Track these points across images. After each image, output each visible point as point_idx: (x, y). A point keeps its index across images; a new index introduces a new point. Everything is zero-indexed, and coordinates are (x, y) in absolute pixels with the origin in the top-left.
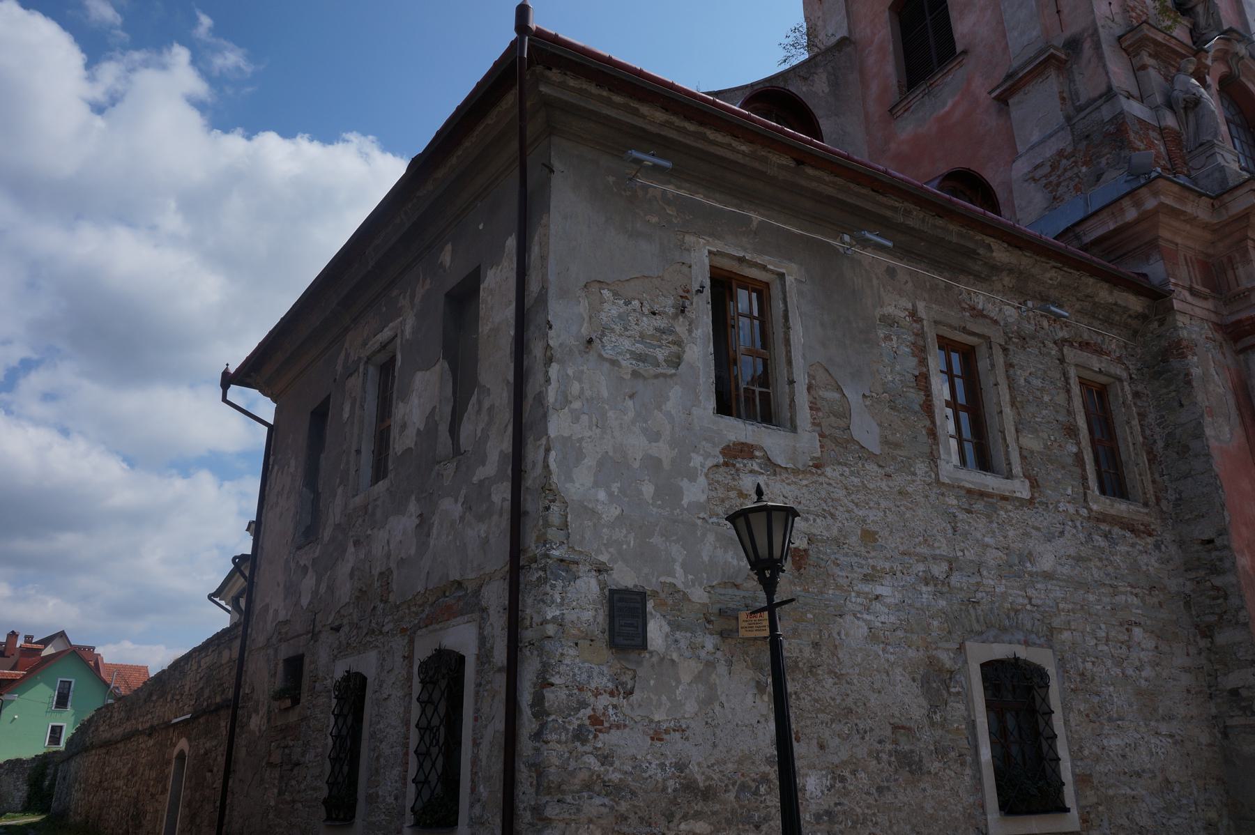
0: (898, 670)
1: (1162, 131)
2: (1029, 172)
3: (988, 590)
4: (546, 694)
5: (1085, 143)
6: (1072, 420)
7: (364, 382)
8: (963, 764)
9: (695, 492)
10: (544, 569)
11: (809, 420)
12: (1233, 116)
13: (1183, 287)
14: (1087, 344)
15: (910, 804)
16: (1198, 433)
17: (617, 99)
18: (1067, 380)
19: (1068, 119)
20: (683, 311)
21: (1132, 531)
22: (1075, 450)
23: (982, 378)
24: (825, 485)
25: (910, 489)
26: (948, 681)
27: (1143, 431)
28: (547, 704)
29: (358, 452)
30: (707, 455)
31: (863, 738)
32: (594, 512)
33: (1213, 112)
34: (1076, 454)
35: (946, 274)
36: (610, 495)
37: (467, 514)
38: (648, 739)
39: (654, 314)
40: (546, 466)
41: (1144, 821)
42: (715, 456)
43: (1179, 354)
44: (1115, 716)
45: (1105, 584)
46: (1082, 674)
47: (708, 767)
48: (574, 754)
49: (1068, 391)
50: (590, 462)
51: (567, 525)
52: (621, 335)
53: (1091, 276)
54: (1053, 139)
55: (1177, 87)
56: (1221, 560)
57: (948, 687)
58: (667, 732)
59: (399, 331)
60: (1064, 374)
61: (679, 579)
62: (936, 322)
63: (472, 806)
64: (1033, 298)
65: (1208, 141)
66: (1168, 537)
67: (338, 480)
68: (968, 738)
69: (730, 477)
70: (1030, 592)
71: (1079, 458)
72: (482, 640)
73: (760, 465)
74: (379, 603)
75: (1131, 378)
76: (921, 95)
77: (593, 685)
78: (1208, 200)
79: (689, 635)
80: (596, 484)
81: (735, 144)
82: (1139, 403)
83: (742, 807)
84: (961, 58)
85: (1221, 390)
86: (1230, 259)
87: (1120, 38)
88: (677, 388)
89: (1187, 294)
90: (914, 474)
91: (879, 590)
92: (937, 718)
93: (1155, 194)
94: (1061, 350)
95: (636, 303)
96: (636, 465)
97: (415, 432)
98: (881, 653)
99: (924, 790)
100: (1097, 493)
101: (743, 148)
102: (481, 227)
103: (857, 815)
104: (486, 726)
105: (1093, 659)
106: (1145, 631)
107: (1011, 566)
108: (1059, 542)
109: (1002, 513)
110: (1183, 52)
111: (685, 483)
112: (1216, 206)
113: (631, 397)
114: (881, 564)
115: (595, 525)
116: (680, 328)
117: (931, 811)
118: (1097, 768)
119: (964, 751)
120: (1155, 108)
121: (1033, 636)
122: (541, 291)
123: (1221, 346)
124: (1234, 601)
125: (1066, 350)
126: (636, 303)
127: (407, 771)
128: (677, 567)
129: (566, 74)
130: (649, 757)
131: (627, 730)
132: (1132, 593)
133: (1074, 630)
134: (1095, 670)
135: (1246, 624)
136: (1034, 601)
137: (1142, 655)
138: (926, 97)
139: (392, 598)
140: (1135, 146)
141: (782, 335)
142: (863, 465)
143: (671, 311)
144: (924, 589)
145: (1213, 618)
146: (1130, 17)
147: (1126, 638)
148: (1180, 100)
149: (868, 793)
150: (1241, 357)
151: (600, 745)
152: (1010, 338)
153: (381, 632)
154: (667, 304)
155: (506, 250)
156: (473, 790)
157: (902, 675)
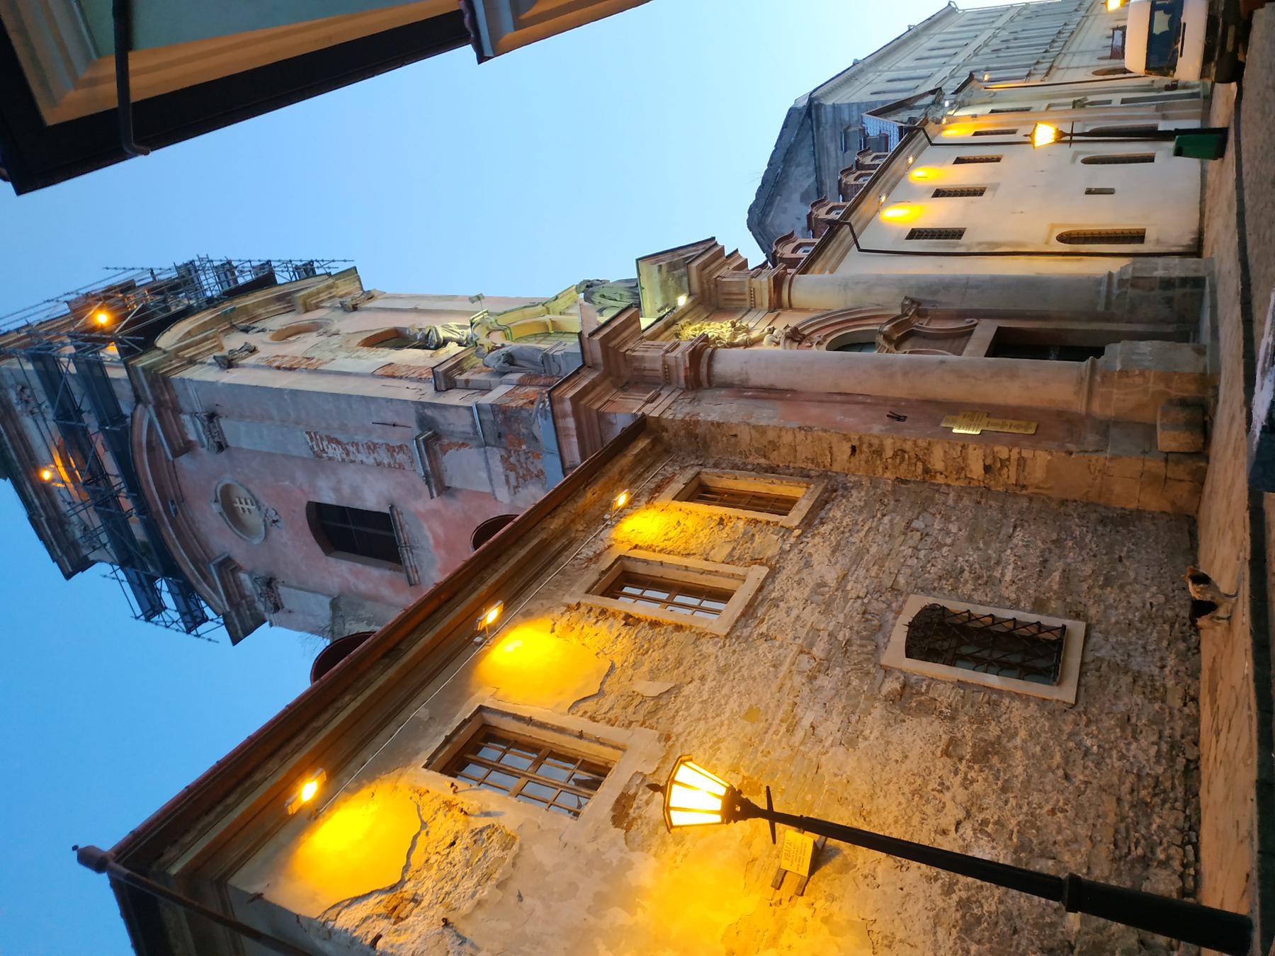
1: (521, 384)
5: (503, 440)
11: (622, 730)
13: (643, 406)
15: (1027, 765)
16: (762, 431)
21: (827, 502)
24: (689, 738)
26: (914, 692)
30: (614, 843)
31: (948, 788)
35: (551, 570)
39: (453, 844)
41: (1087, 569)
46: (940, 578)
53: (605, 464)
54: (490, 462)
56: (870, 445)
57: (922, 694)
62: (587, 592)
64: (603, 513)
68: (973, 692)
69: (643, 827)
70: (853, 594)
79: (787, 931)
82: (724, 466)
83: (990, 940)
85: (734, 406)
86: (636, 369)
87: (436, 389)
89: (649, 405)
91: (806, 723)
93: (562, 400)
98: (867, 743)
99: (1016, 748)
101: (347, 698)
103: (1026, 821)
108: (816, 559)
109: (773, 595)
114: (780, 715)
117: (1038, 748)
118: (1031, 591)
119: (986, 699)
124: (908, 446)
129: (176, 841)
132: (880, 519)
136: (861, 595)
137: (937, 526)
138: (414, 551)
141: (535, 729)
144: (817, 683)
145: (920, 465)
147: (919, 534)
149: (1006, 802)
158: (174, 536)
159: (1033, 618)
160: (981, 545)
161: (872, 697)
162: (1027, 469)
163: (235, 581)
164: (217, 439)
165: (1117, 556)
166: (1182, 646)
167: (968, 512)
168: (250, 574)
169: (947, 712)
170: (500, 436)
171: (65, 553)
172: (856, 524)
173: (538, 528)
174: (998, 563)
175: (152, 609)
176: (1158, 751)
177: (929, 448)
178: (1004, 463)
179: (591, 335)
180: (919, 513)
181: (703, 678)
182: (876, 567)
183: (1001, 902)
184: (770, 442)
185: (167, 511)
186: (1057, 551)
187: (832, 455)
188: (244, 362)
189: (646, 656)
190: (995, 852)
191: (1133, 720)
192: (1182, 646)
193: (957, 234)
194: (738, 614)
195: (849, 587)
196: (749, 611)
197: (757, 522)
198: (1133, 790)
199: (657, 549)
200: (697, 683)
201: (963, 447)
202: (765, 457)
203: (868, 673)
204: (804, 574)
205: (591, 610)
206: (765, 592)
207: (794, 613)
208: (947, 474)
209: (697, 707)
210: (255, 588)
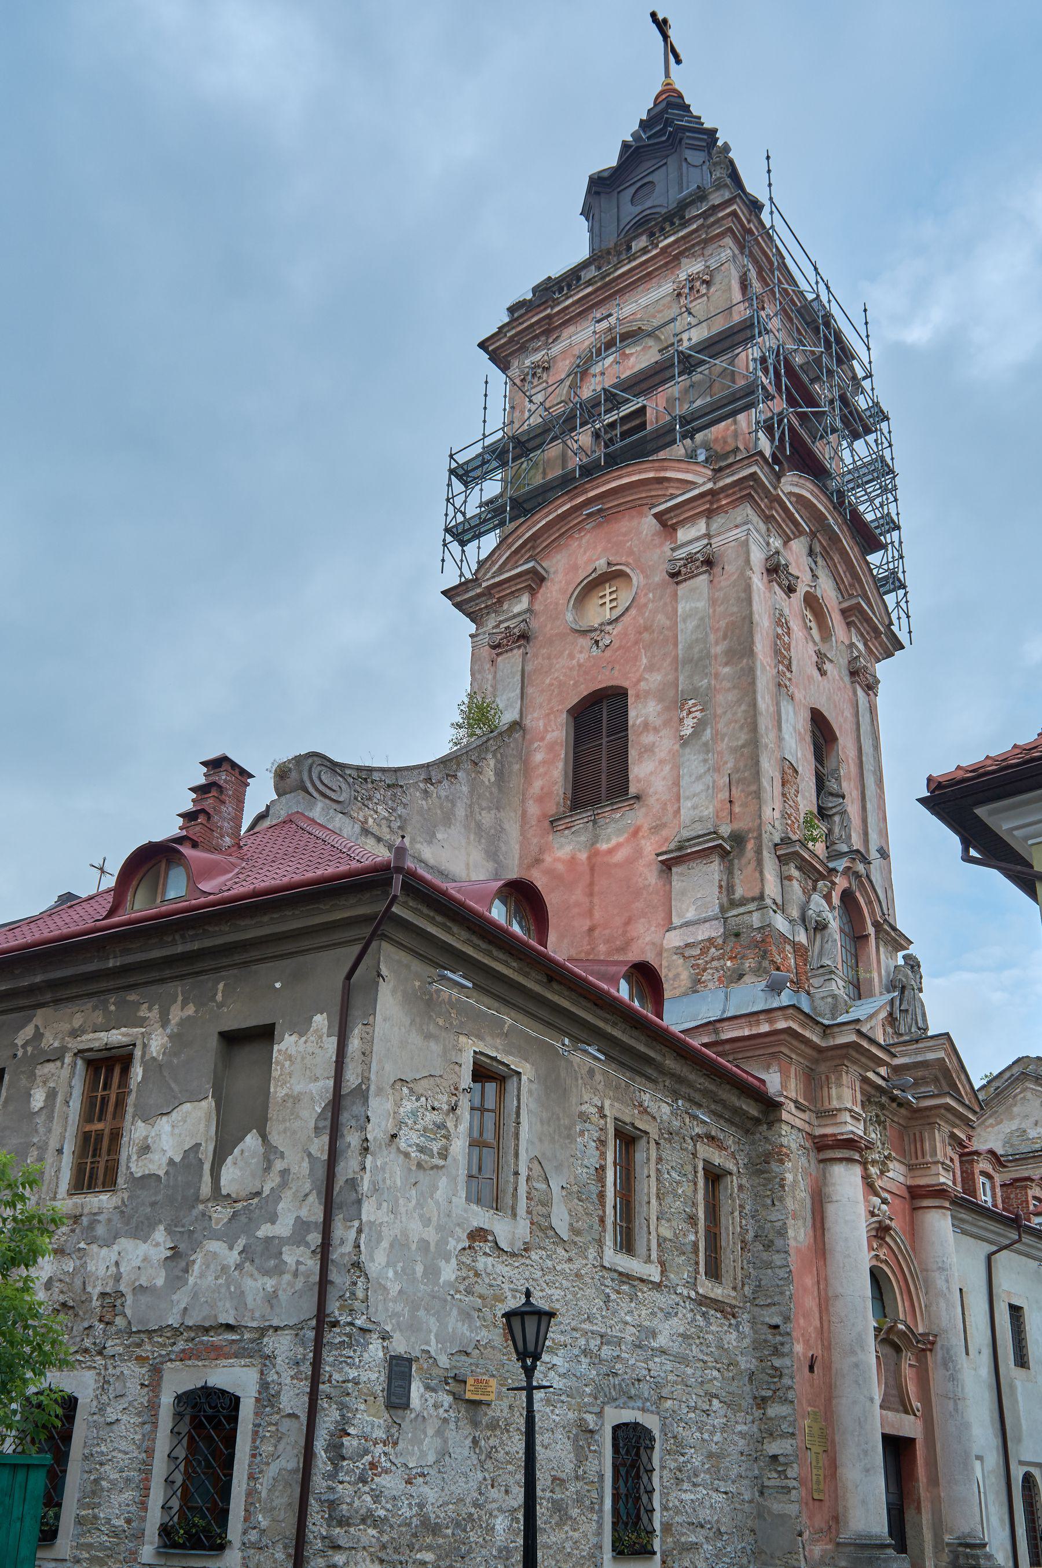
7: (73, 1074)
9: (449, 1272)
10: (350, 1336)
14: (713, 1138)
16: (782, 1233)
17: (439, 919)
18: (696, 1172)
20: (453, 1109)
21: (722, 1312)
22: (692, 1238)
23: (637, 1168)
25: (583, 1272)
30: (459, 1240)
32: (385, 1288)
36: (396, 1273)
37: (247, 1264)
39: (433, 1109)
49: (695, 1184)
50: (385, 1244)
56: (782, 1344)
59: (139, 1043)
64: (683, 1098)
70: (651, 1364)
72: (264, 1385)
73: (490, 1247)
79: (434, 1394)
80: (388, 1265)
85: (803, 1194)
88: (444, 1178)
90: (586, 1258)
91: (556, 1360)
95: (423, 1099)
96: (414, 1247)
97: (165, 1161)
99: (567, 1532)
101: (515, 964)
102: (278, 985)
104: (268, 1464)
111: (442, 1264)
116: (450, 1124)
119: (595, 1501)
122: (360, 1085)
124: (786, 1381)
126: (423, 1099)
128: (432, 1337)
132: (715, 1368)
135: (792, 1402)
137: (716, 1422)
139: (119, 1321)
143: (445, 1107)
145: (770, 1393)
147: (708, 1407)
151: (374, 1487)
154: (443, 1101)
159: (657, 1525)
160: (706, 1466)
161: (581, 1408)
162: (779, 1496)
167: (733, 1447)
169: (580, 1472)
172: (708, 1347)
173: (665, 1049)
174: (695, 1485)
177: (786, 1401)
178: (782, 1474)
180: (724, 1402)
181: (570, 1260)
182: (675, 1378)
183: (476, 1543)
184: (772, 1241)
186: (711, 1534)
187: (767, 1305)
189: (576, 1201)
190: (502, 1532)
193: (1022, 1360)
194: (620, 1269)
195: (656, 1359)
196: (625, 1277)
197: (696, 1251)
199: (659, 1167)
200: (566, 1255)
201: (793, 1434)
202: (756, 1236)
203: (596, 1398)
204: (660, 1315)
205: (601, 1129)
206: (641, 1286)
207: (628, 1318)
208: (764, 1420)
209: (549, 1263)
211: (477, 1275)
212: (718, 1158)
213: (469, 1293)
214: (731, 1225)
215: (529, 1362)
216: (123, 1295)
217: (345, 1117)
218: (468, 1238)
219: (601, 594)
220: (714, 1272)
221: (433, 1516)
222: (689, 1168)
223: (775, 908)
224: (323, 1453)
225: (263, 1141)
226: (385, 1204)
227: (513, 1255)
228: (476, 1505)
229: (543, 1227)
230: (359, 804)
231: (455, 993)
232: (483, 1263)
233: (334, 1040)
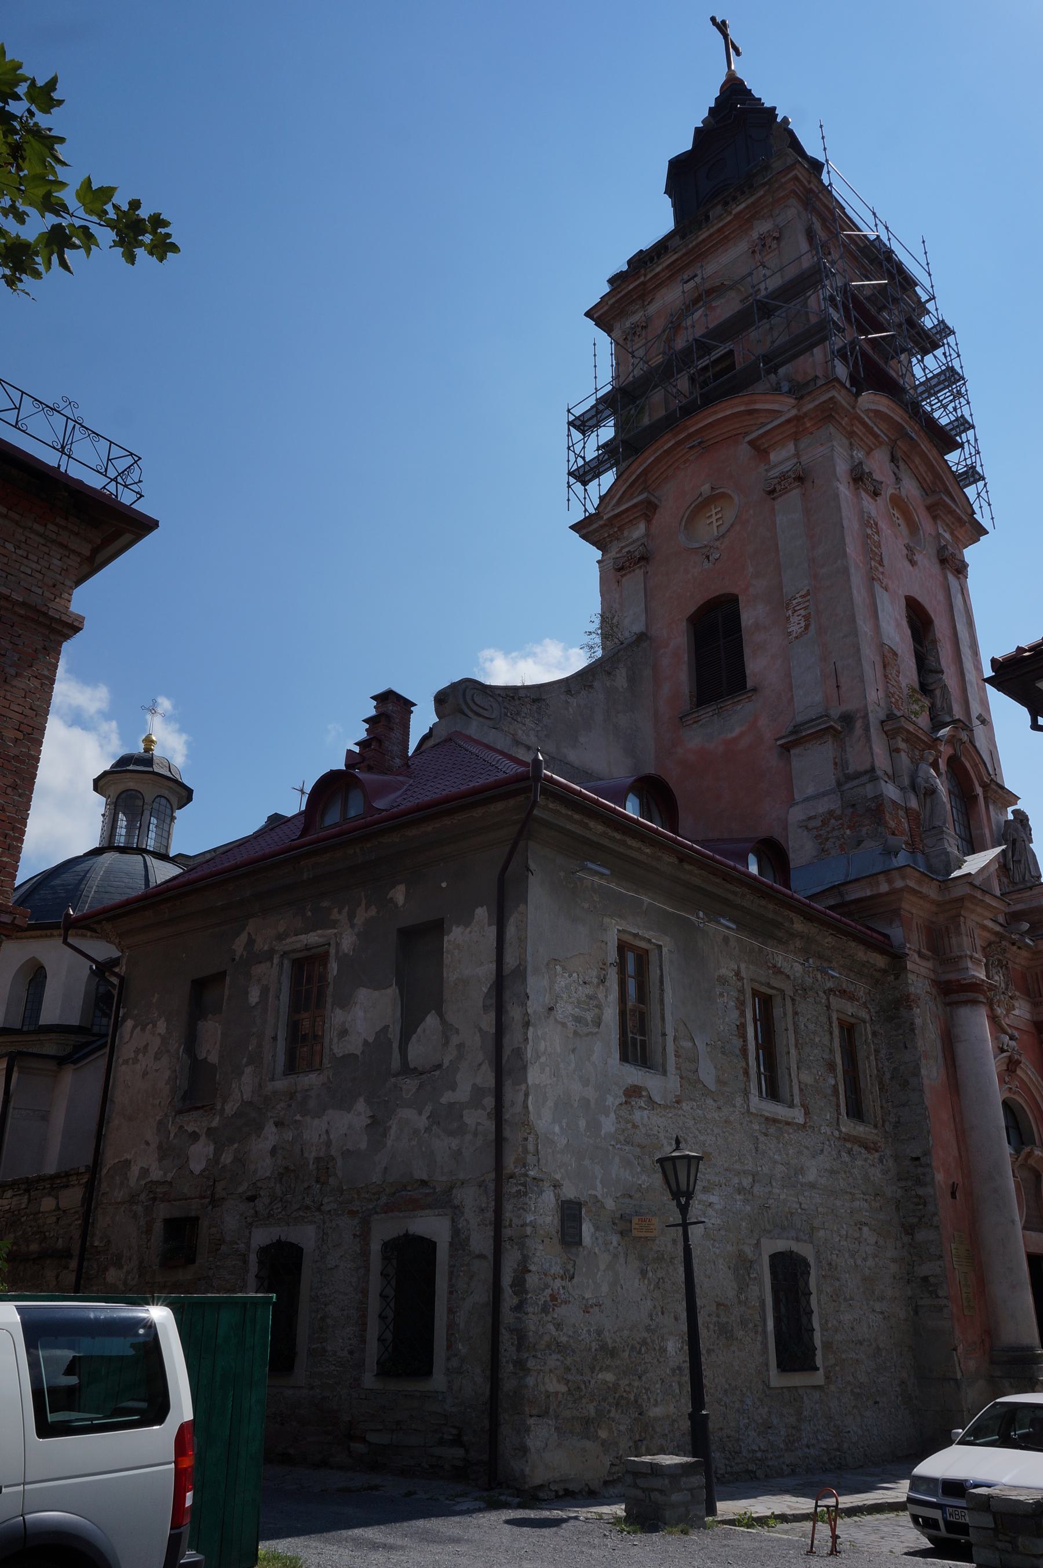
0: (721, 1261)
1: (907, 810)
2: (803, 820)
3: (775, 1197)
4: (527, 1279)
5: (851, 810)
6: (832, 1058)
8: (756, 1332)
9: (608, 1125)
12: (953, 787)
13: (914, 951)
16: (916, 1072)
17: (576, 816)
18: (831, 1023)
19: (839, 784)
20: (603, 982)
21: (866, 1148)
22: (833, 1082)
25: (732, 1119)
27: (877, 1065)
28: (527, 1286)
29: (275, 1038)
33: (944, 803)
34: (834, 1086)
36: (561, 1128)
37: (435, 1127)
38: (582, 1312)
39: (585, 983)
40: (525, 1106)
42: (620, 1097)
43: (908, 1006)
44: (848, 1297)
45: (847, 1192)
46: (830, 1264)
47: (614, 1333)
48: (542, 1322)
49: (831, 1033)
50: (550, 1103)
51: (538, 1152)
52: (566, 1002)
54: (826, 799)
55: (921, 774)
58: (591, 1306)
59: (333, 942)
60: (829, 1018)
61: (599, 1191)
62: (751, 979)
63: (448, 1359)
65: (939, 826)
66: (888, 1152)
67: (245, 1059)
69: (628, 1112)
70: (801, 1199)
71: (835, 1088)
72: (456, 1232)
73: (644, 1102)
74: (313, 1183)
75: (872, 1019)
76: (711, 714)
77: (553, 1272)
78: (937, 883)
79: (603, 1234)
81: (643, 847)
84: (750, 695)
85: (933, 1036)
87: (882, 722)
89: (916, 956)
90: (734, 1106)
91: (713, 1199)
92: (743, 1297)
93: (903, 878)
94: (828, 999)
95: (575, 975)
96: (576, 1105)
99: (734, 1352)
100: (846, 1117)
101: (648, 851)
102: (444, 885)
105: (837, 1252)
106: (870, 1229)
107: (790, 1178)
109: (786, 1135)
110: (926, 740)
111: (603, 1119)
112: (942, 888)
113: (573, 1051)
115: (553, 1152)
117: (737, 1368)
120: (902, 789)
121: (802, 1233)
123: (935, 998)
125: (831, 997)
126: (575, 975)
127: (365, 1330)
128: (598, 1183)
129: (548, 799)
130: (582, 1325)
131: (570, 1305)
133: (827, 1229)
134: (838, 1261)
135: (937, 1227)
136: (803, 1206)
138: (716, 716)
139: (331, 1180)
140: (889, 826)
142: (705, 1100)
143: (595, 981)
144: (738, 1197)
145: (915, 1220)
146: (891, 702)
148: (922, 787)
150: (948, 1008)
151: (556, 1316)
152: (797, 990)
153: (319, 1209)
154: (593, 975)
155: (476, 916)
156: (449, 1347)
157: (723, 1264)
158: (665, 448)
159: (818, 1342)
160: (861, 1290)
163: (634, 519)
164: (778, 488)
165: (878, 1400)
166: (825, 1459)
168: (647, 534)
169: (743, 1297)
170: (854, 805)
171: (612, 306)
175: (583, 424)
176: (756, 1451)
179: (971, 884)
185: (690, 436)
188: (864, 494)
191: (770, 1431)
192: (825, 1459)
194: (767, 1114)
198: (728, 1437)
202: (892, 1078)
203: (752, 1231)
204: (805, 1151)
206: (786, 1127)
210: (634, 542)
211: (635, 1126)
212: (850, 1008)
213: (628, 1143)
214: (868, 1068)
215: (683, 1200)
216: (334, 1159)
217: (507, 995)
218: (624, 1094)
219: (709, 514)
220: (856, 1112)
221: (609, 1341)
222: (823, 1019)
223: (887, 780)
224: (509, 1288)
225: (441, 1020)
226: (547, 1069)
227: (666, 1107)
228: (648, 1329)
229: (690, 1081)
230: (509, 719)
231: (596, 879)
232: (637, 1116)
233: (494, 928)
